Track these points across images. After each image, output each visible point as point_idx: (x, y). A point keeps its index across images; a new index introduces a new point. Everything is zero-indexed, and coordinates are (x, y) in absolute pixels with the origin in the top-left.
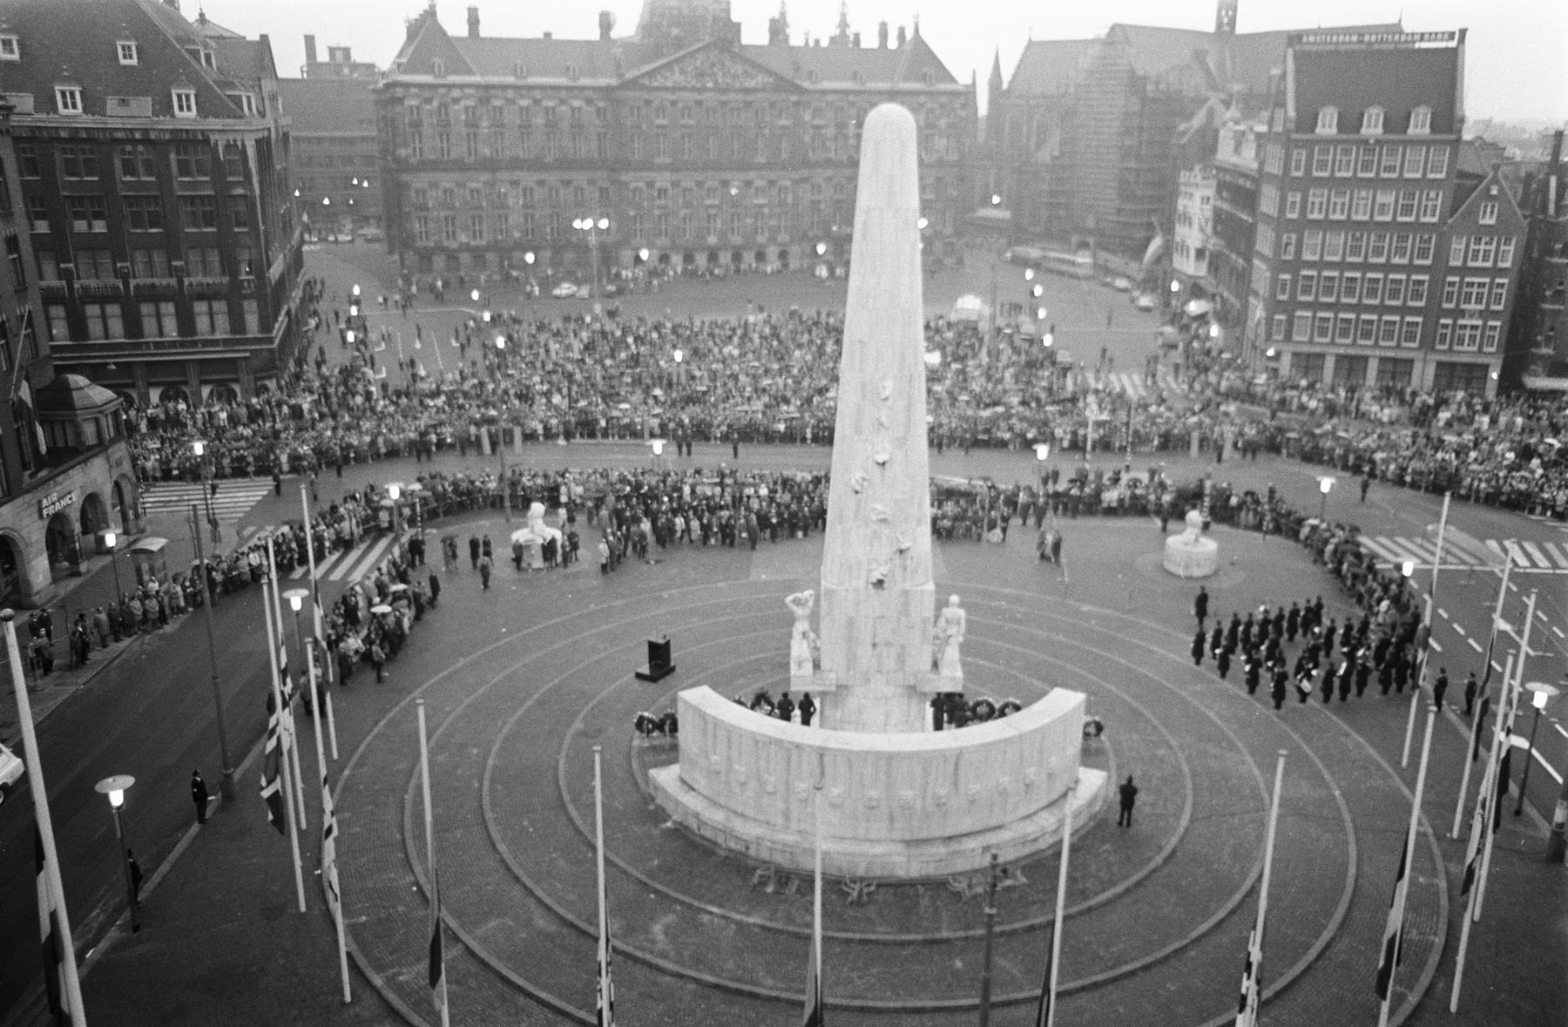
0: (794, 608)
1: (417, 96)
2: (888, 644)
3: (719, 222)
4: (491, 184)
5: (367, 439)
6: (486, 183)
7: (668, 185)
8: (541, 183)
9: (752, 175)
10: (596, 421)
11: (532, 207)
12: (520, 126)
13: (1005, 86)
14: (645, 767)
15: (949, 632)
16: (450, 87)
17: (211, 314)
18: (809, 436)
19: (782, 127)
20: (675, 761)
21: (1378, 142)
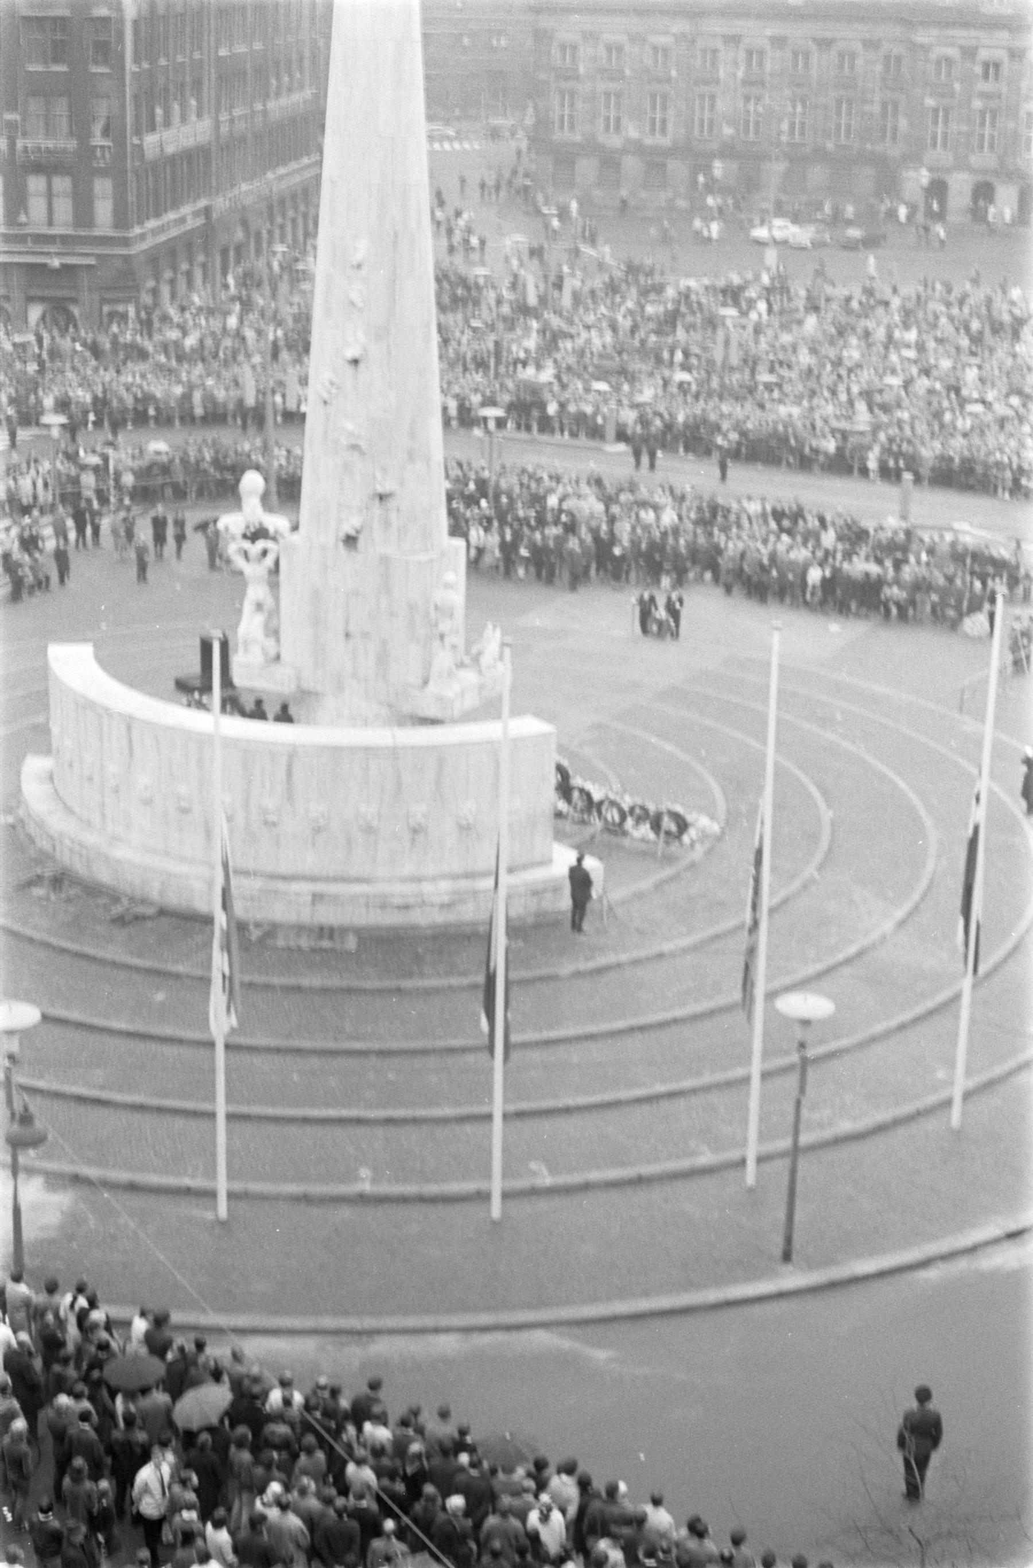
2: (365, 635)
5: (178, 390)
6: (680, 38)
10: (542, 406)
17: (50, 195)
18: (872, 464)
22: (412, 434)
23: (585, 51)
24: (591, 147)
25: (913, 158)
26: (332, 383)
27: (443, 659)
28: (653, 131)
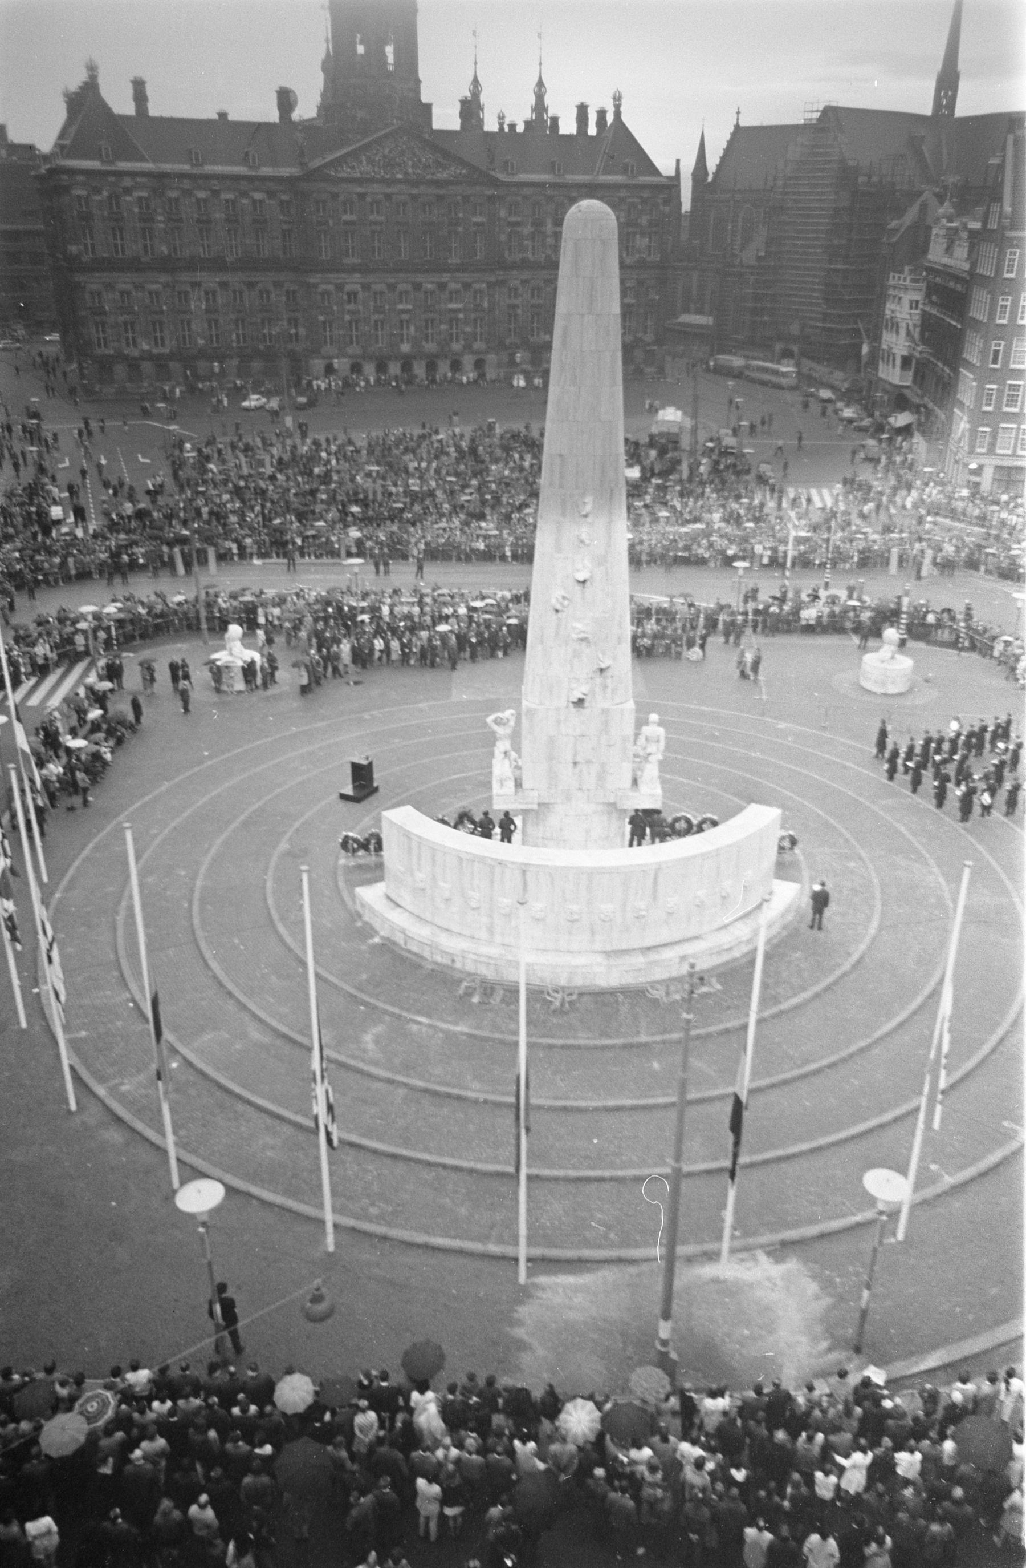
0: (496, 728)
2: (588, 762)
3: (412, 328)
6: (166, 285)
8: (224, 285)
9: (445, 277)
11: (216, 311)
12: (199, 221)
13: (710, 179)
14: (352, 885)
15: (649, 750)
16: (120, 174)
18: (508, 554)
20: (381, 879)
24: (121, 357)
25: (315, 352)
26: (564, 598)
28: (156, 344)
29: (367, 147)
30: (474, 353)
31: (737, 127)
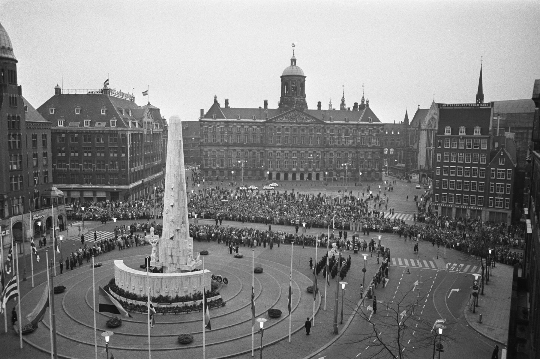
1: (207, 124)
4: (227, 150)
6: (226, 150)
7: (280, 152)
9: (308, 149)
19: (318, 135)
21: (463, 138)
22: (183, 218)
23: (209, 153)
24: (210, 169)
27: (189, 259)
29: (286, 114)
30: (315, 171)
31: (419, 109)
